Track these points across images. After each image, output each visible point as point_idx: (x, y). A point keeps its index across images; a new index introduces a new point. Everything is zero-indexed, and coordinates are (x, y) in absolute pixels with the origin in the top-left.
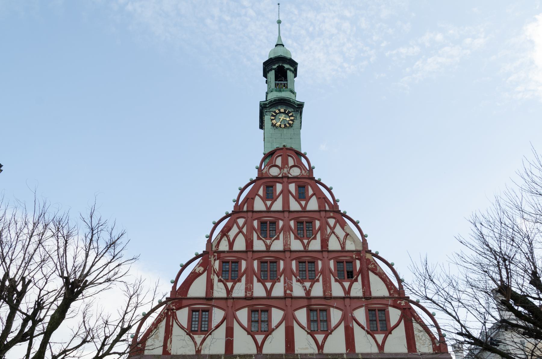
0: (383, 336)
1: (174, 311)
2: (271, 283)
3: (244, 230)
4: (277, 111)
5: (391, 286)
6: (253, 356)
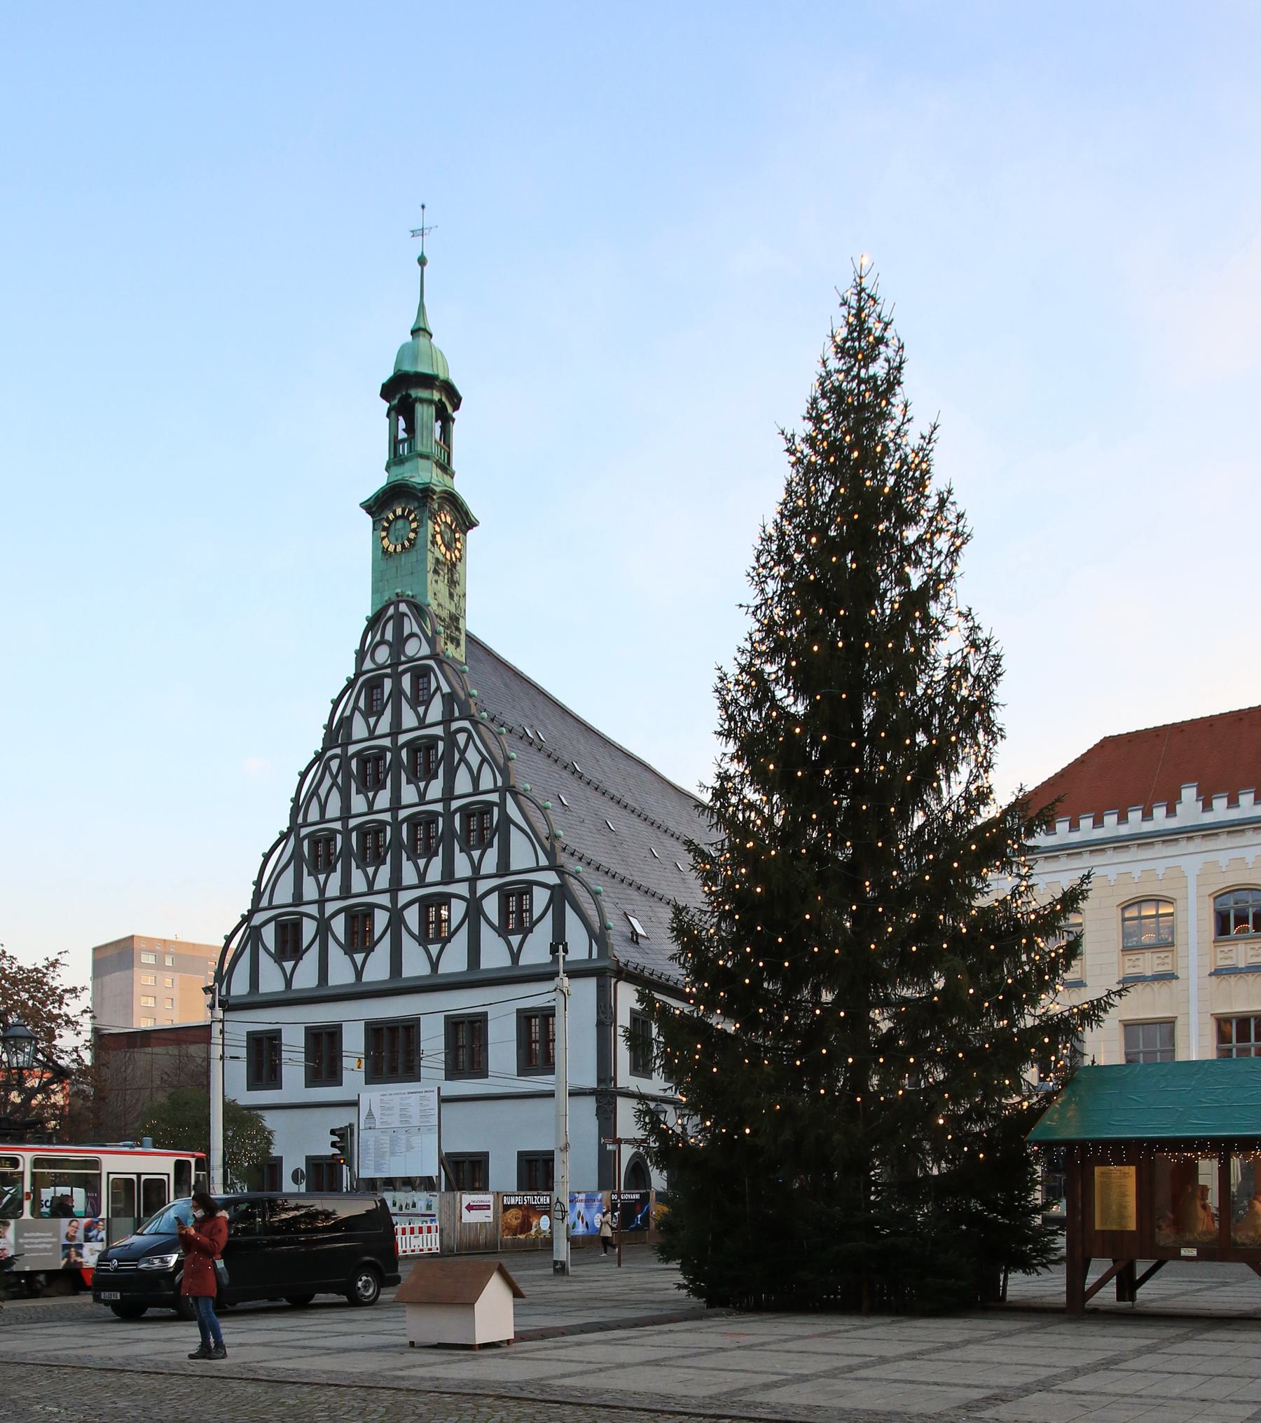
4: (391, 516)
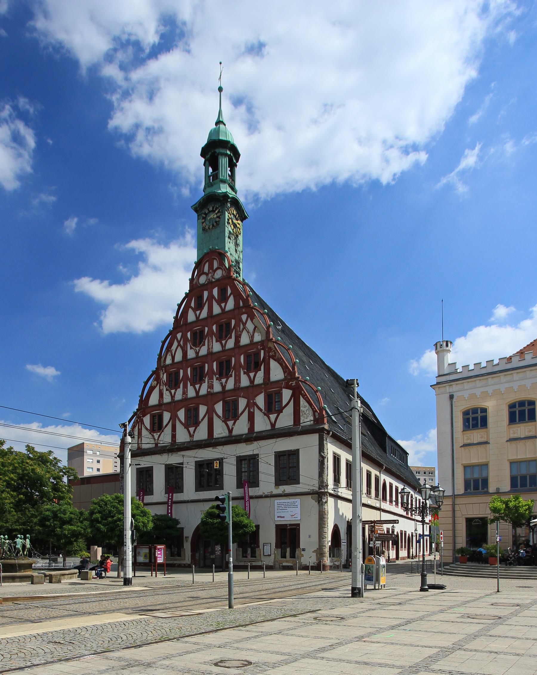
3: (182, 343)
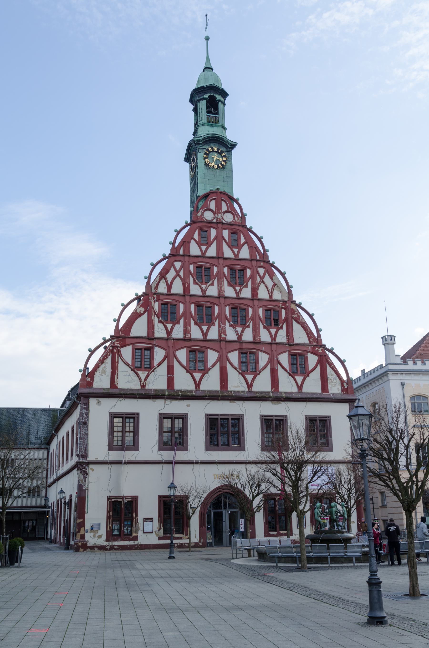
0: (302, 378)
1: (119, 348)
2: (207, 327)
3: (181, 273)
4: (210, 149)
5: (311, 335)
6: (193, 392)
